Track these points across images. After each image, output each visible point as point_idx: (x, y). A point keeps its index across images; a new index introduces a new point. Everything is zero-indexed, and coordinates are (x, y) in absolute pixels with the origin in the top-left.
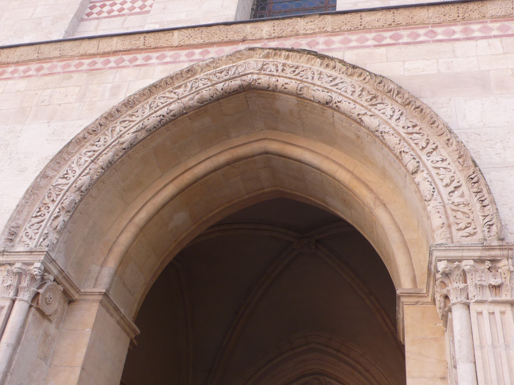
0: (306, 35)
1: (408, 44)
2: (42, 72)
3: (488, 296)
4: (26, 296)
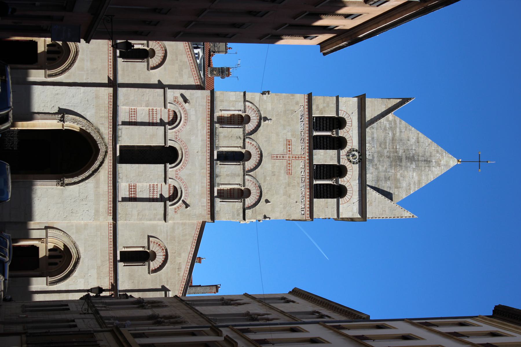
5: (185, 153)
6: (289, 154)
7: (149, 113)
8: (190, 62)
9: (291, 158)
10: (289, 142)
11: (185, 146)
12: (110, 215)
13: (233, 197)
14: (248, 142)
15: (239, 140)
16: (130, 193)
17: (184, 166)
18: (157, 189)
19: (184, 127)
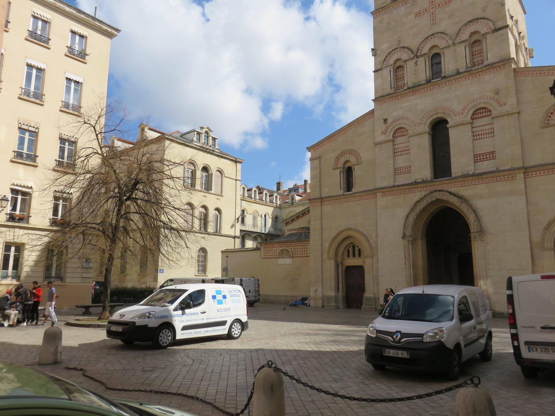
0: (446, 184)
1: (467, 186)
2: (393, 194)
3: (480, 240)
4: (410, 244)
5: (436, 111)
6: (429, 9)
7: (399, 155)
8: (352, 128)
9: (433, 6)
10: (417, 15)
11: (428, 113)
12: (515, 177)
13: (482, 49)
14: (420, 53)
15: (418, 63)
16: (485, 159)
17: (449, 109)
18: (479, 131)
19: (409, 119)
